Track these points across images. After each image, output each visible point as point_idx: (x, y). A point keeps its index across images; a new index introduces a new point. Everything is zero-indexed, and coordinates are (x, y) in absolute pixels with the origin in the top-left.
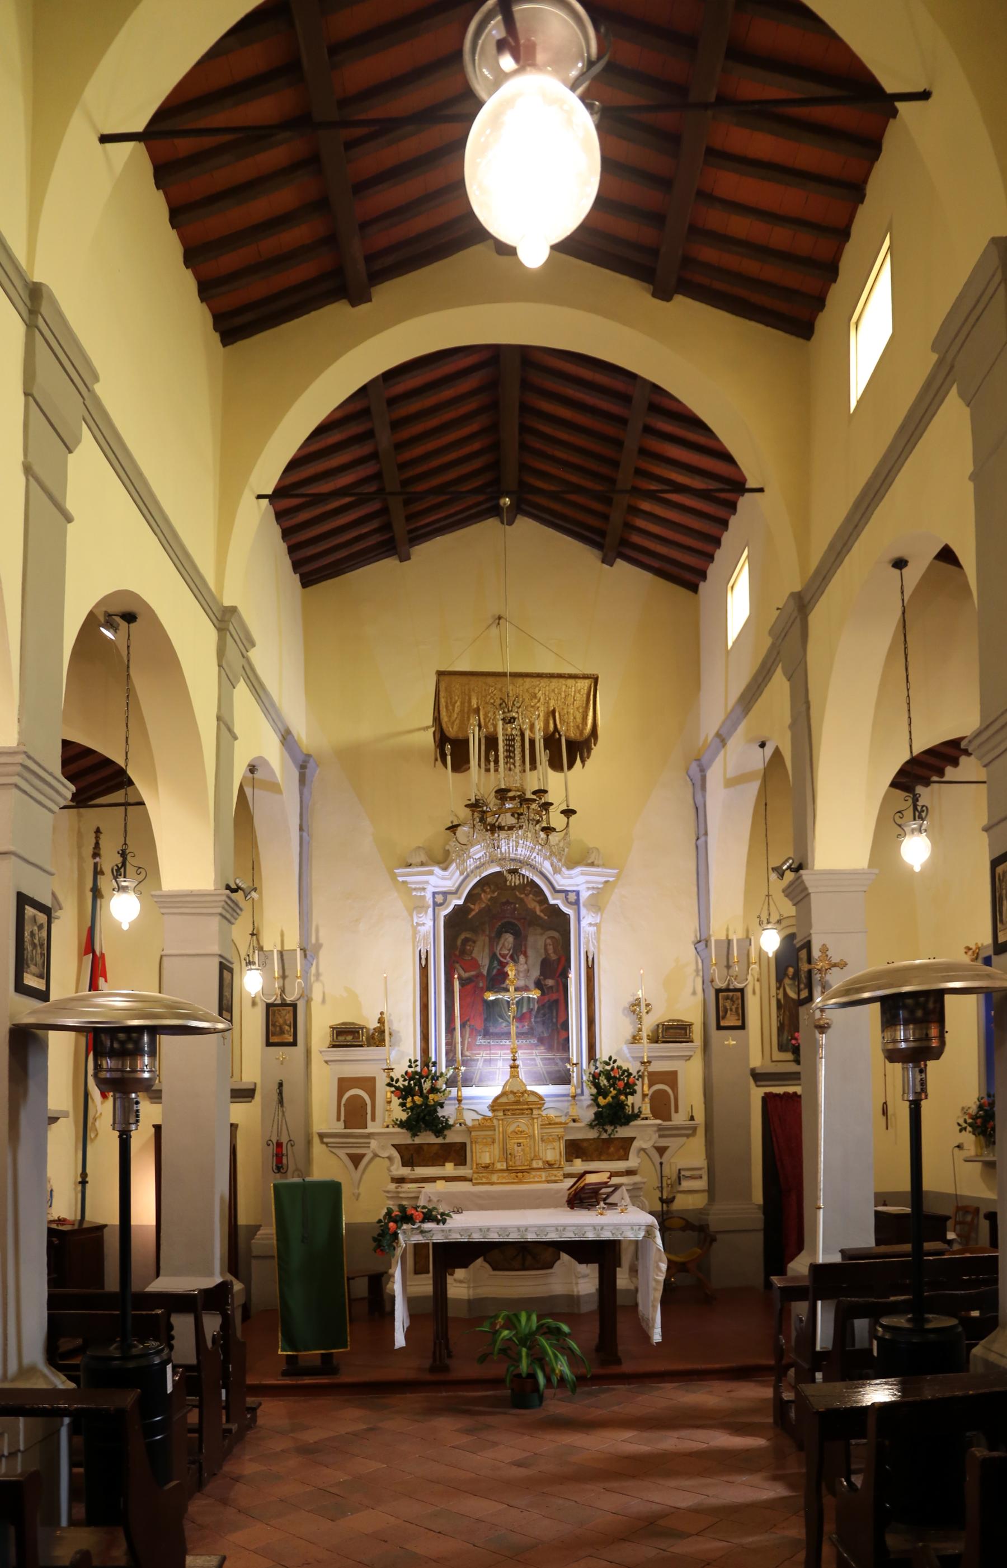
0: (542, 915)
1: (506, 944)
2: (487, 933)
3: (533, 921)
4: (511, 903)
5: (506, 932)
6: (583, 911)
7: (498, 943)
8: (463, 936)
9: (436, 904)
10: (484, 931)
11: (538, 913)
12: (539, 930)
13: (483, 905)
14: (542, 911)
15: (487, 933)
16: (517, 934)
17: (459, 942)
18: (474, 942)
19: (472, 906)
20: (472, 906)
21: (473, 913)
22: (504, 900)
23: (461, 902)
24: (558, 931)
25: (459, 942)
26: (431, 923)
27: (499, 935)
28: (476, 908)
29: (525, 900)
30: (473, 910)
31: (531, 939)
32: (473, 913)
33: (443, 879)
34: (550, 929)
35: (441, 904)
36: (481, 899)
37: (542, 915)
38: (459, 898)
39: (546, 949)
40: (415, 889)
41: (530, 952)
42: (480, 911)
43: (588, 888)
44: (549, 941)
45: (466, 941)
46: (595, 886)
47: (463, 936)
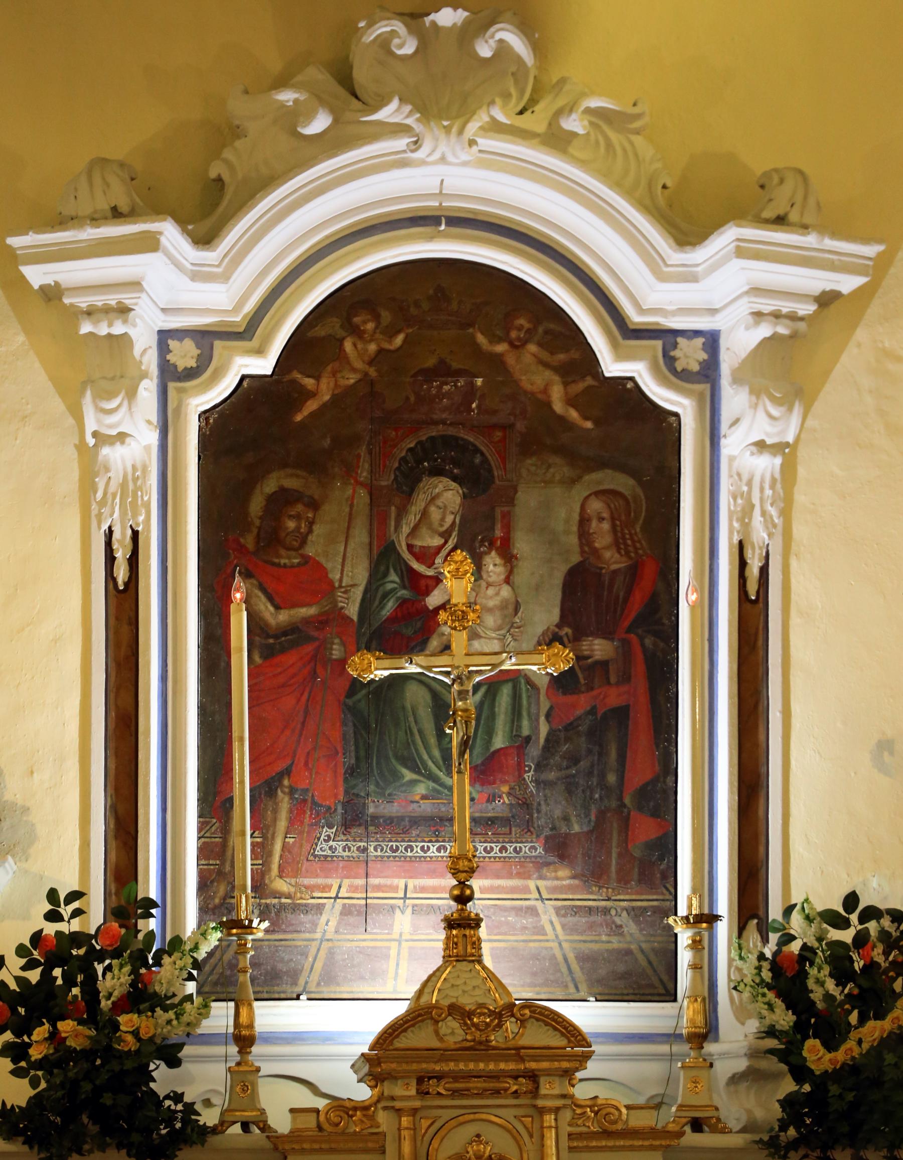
0: (573, 414)
1: (435, 514)
2: (364, 474)
3: (541, 436)
4: (459, 373)
5: (437, 472)
6: (734, 399)
7: (402, 511)
8: (270, 486)
9: (169, 374)
10: (350, 470)
11: (558, 407)
12: (560, 468)
13: (352, 379)
14: (571, 402)
15: (364, 474)
16: (475, 481)
17: (256, 506)
18: (314, 505)
19: (309, 382)
20: (309, 382)
21: (312, 406)
22: (431, 362)
23: (264, 365)
24: (634, 473)
25: (256, 506)
26: (152, 438)
27: (408, 481)
28: (323, 389)
29: (510, 360)
30: (312, 395)
31: (528, 500)
32: (312, 406)
33: (198, 275)
34: (600, 464)
35: (191, 374)
36: (341, 355)
37: (573, 414)
38: (260, 351)
39: (584, 534)
40: (89, 313)
41: (522, 545)
42: (336, 400)
43: (758, 315)
44: (596, 506)
45: (282, 500)
46: (786, 307)
47: (270, 486)
